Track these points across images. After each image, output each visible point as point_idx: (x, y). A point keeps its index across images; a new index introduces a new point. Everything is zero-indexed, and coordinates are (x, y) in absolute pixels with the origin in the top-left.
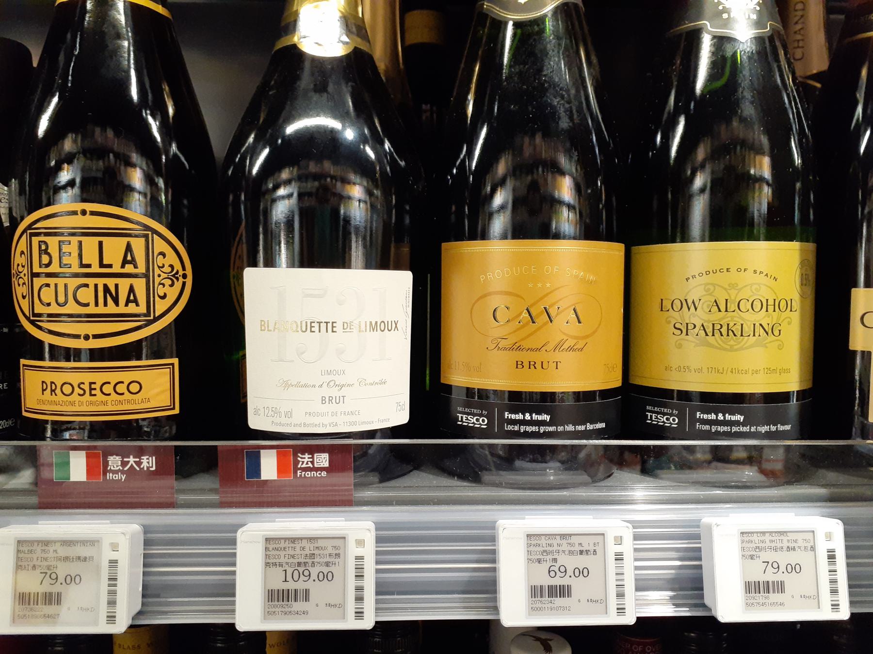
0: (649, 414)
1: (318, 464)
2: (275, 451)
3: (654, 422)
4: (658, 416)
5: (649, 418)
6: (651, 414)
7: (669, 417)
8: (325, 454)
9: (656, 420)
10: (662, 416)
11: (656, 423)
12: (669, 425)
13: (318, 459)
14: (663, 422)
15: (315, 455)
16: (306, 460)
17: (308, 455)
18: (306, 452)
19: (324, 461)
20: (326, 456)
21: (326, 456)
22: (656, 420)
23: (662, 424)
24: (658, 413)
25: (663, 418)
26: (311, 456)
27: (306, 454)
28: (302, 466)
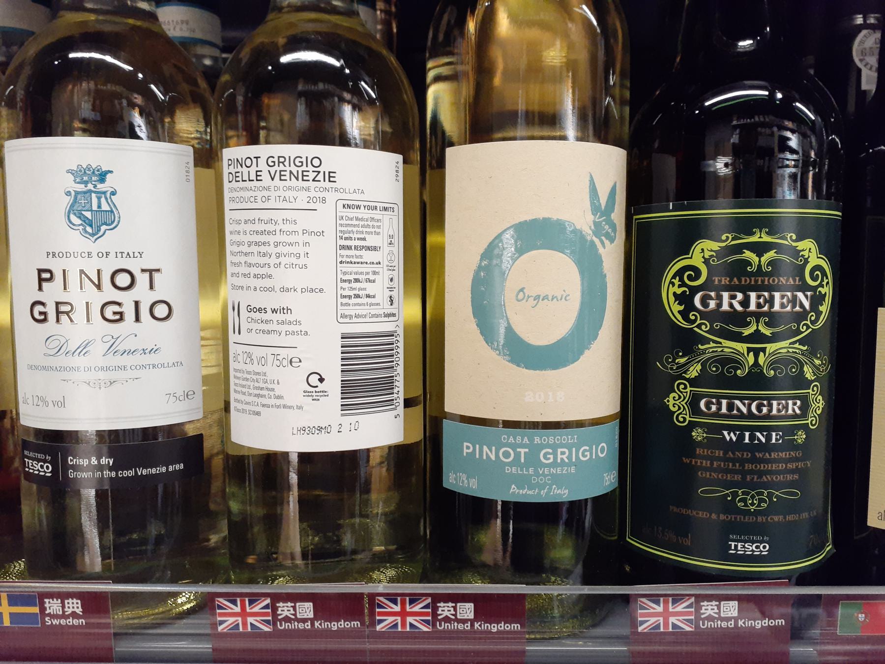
0: (733, 544)
3: (739, 552)
4: (746, 545)
5: (733, 548)
6: (736, 543)
7: (759, 544)
9: (743, 549)
10: (751, 544)
11: (742, 552)
12: (758, 553)
14: (753, 551)
22: (743, 549)
23: (750, 553)
24: (745, 542)
25: (752, 546)
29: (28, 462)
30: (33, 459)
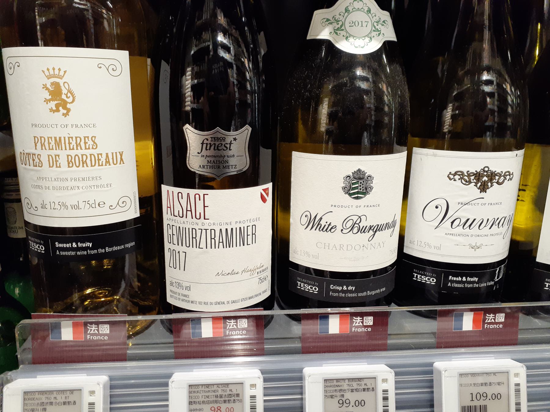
1: (366, 323)
2: (338, 315)
8: (371, 317)
13: (366, 320)
15: (365, 318)
16: (358, 321)
17: (360, 317)
18: (359, 316)
19: (370, 321)
20: (372, 318)
21: (372, 318)
26: (361, 318)
27: (359, 317)
28: (356, 325)
29: (31, 243)
30: (34, 242)
